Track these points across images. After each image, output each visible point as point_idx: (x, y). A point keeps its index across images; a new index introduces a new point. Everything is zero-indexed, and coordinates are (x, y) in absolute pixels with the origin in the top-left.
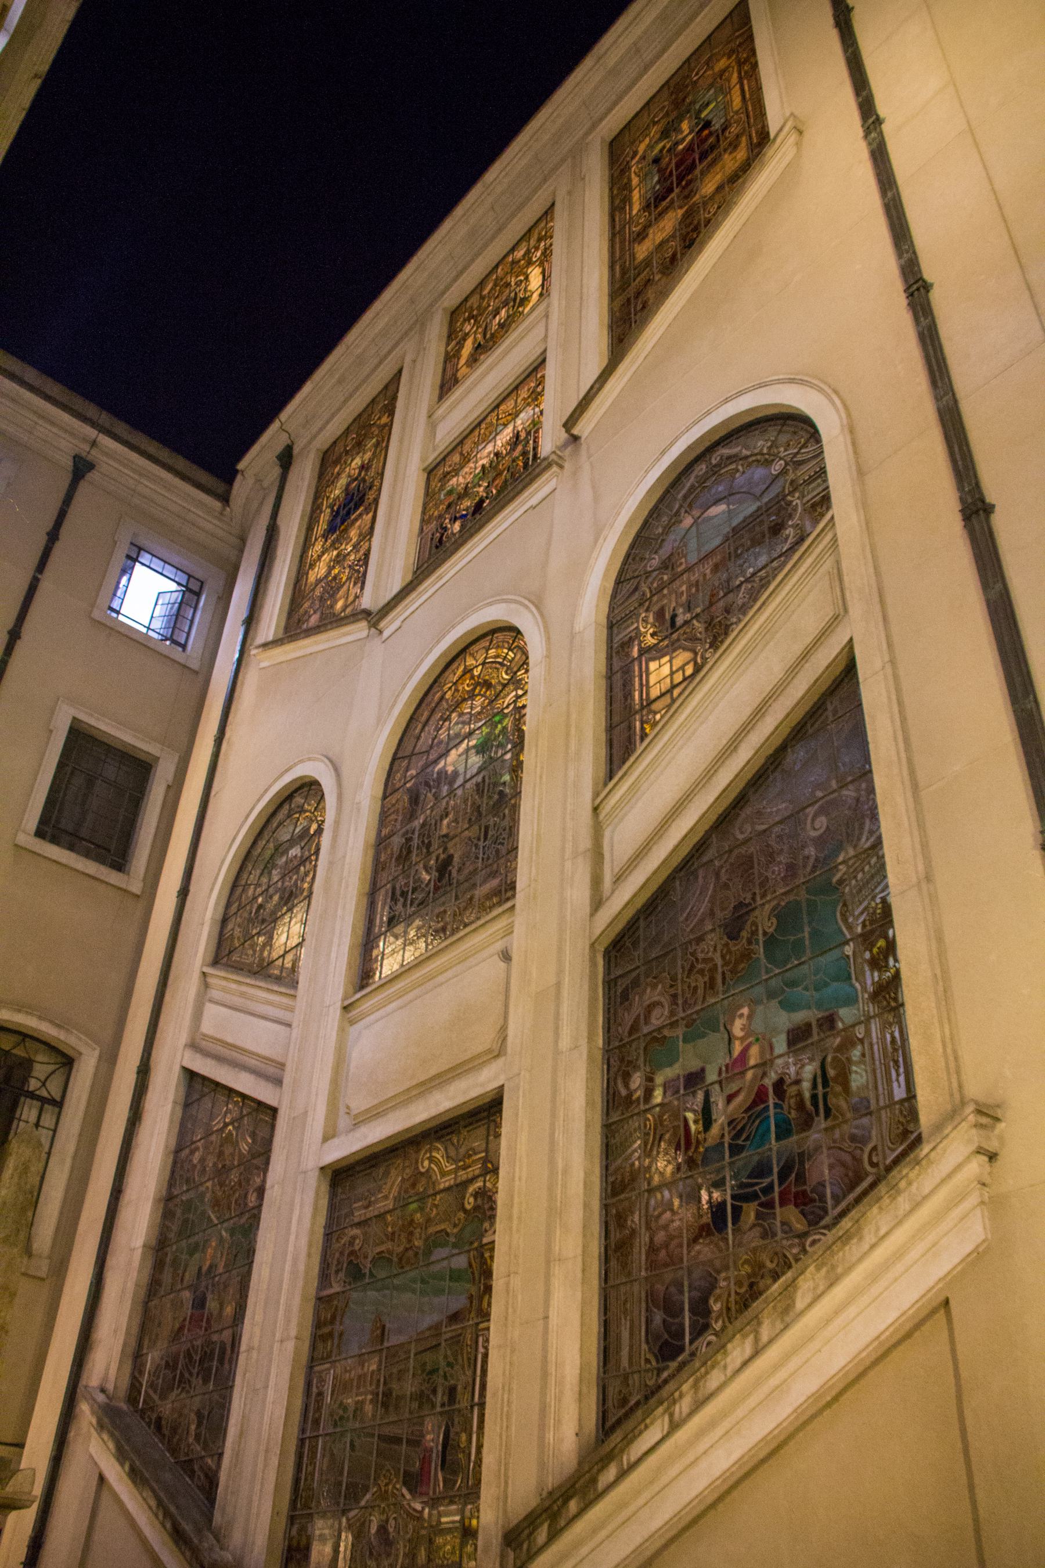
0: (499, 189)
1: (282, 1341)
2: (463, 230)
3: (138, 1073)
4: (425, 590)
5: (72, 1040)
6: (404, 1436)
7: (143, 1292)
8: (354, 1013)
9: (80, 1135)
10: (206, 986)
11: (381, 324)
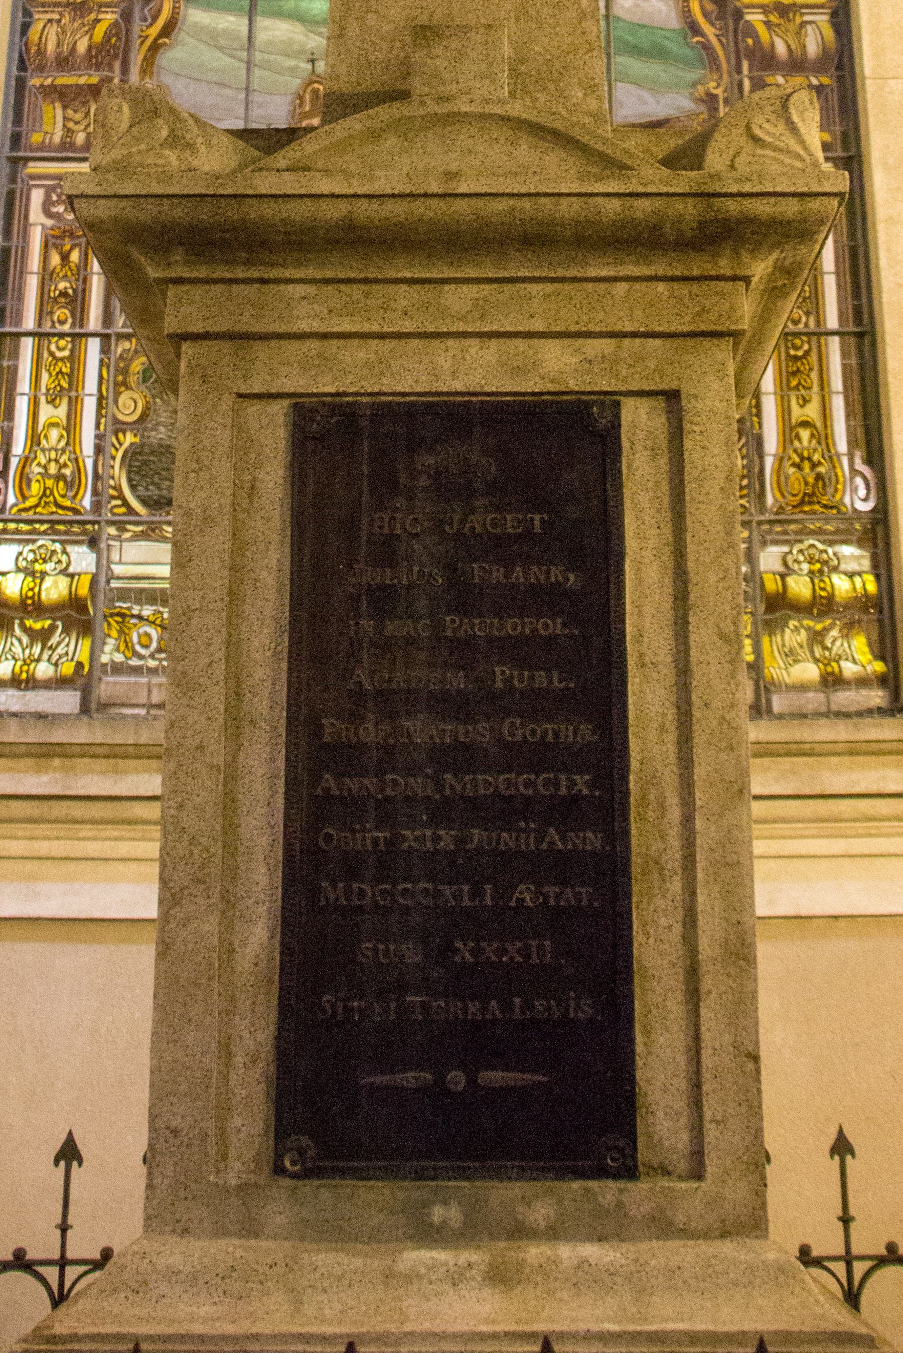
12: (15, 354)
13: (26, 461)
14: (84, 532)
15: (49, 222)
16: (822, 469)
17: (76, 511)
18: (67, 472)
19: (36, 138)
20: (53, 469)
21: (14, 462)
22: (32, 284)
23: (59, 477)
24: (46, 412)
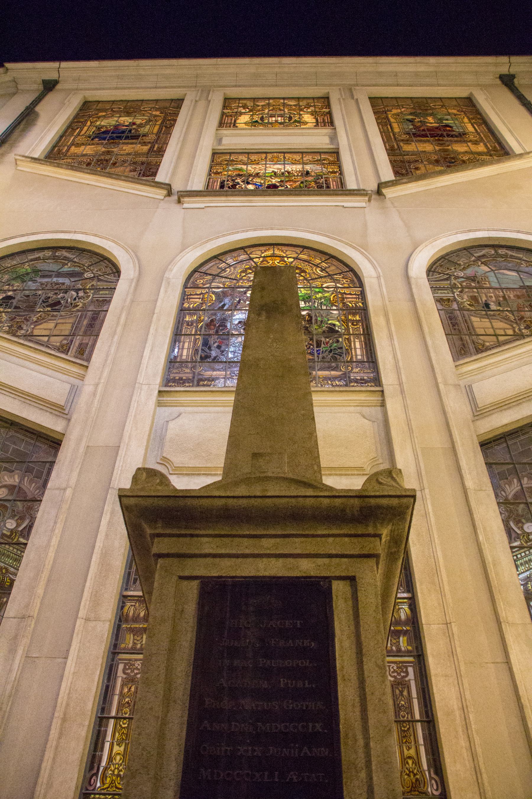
0: (286, 70)
2: (253, 70)
4: (234, 201)
8: (166, 398)
11: (168, 71)
12: (107, 726)
13: (106, 769)
15: (125, 676)
16: (418, 777)
19: (123, 646)
20: (116, 772)
21: (101, 769)
22: (116, 698)
23: (118, 775)
24: (116, 749)
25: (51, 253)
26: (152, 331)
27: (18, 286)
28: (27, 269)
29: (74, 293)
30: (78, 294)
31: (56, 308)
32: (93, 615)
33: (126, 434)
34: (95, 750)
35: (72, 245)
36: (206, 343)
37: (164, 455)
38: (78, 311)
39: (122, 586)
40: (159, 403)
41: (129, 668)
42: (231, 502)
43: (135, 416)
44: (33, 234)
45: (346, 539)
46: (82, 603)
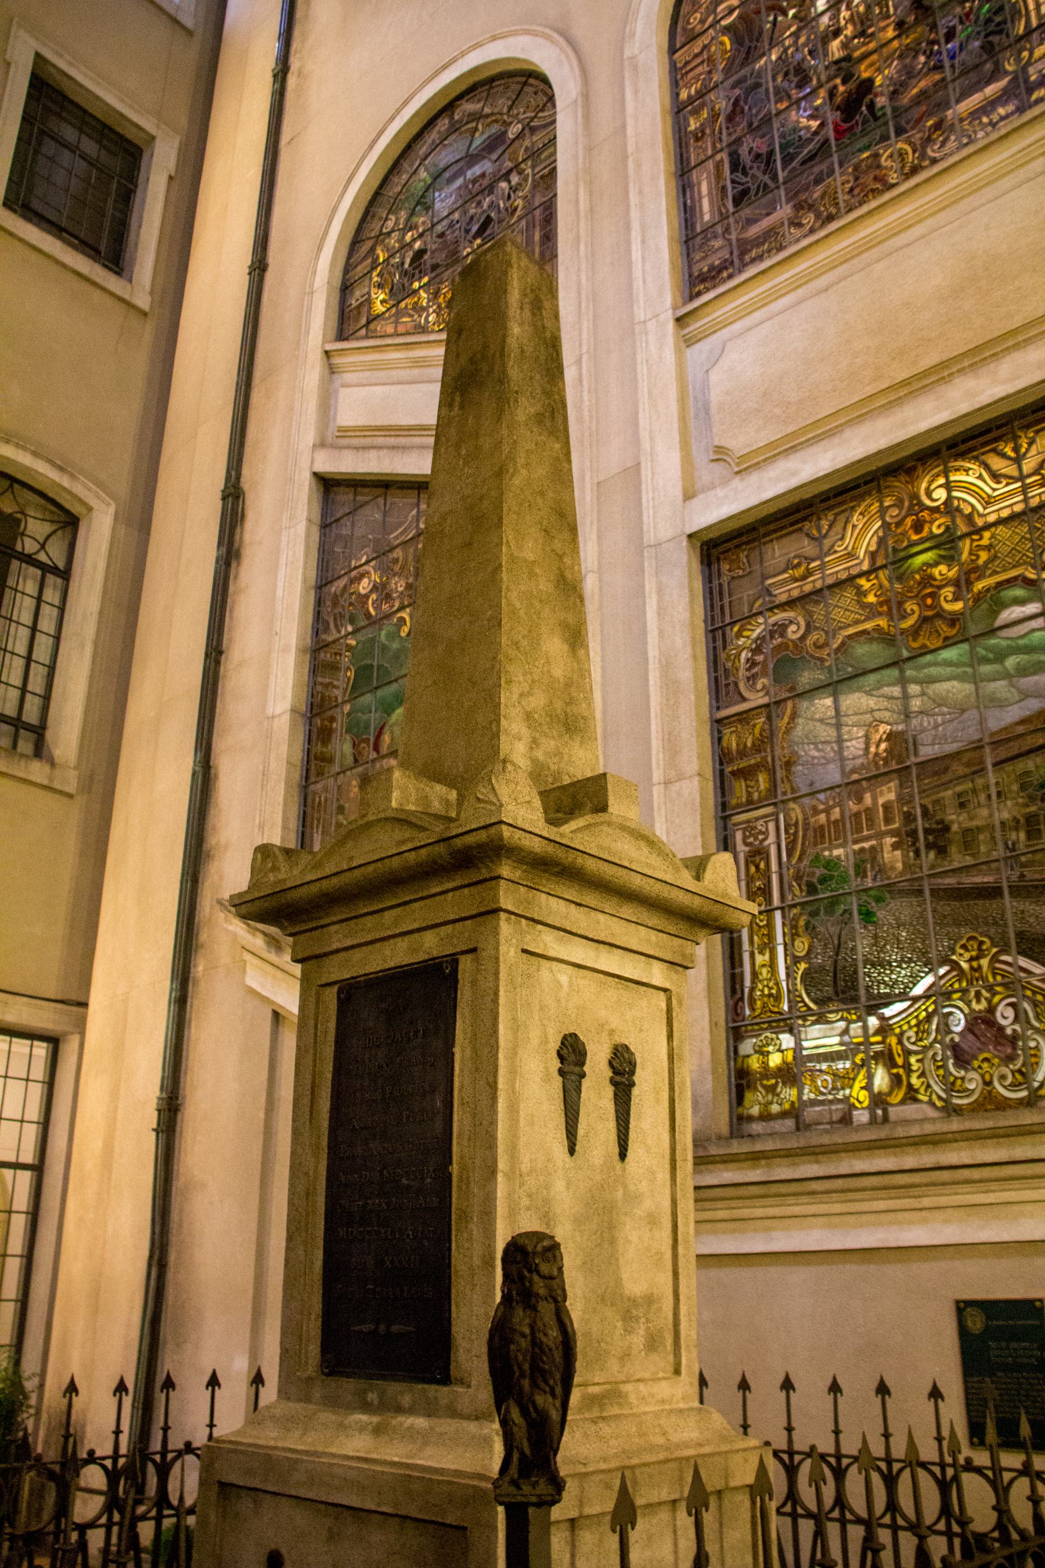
1: (667, 783)
3: (224, 499)
5: (78, 489)
6: (1005, 885)
7: (297, 775)
8: (695, 326)
9: (101, 613)
10: (332, 370)
13: (752, 989)
14: (786, 1025)
15: (747, 849)
17: (780, 1013)
18: (774, 991)
19: (734, 802)
20: (766, 991)
21: (746, 991)
23: (770, 995)
24: (760, 959)
25: (447, 121)
26: (633, 198)
27: (424, 223)
28: (424, 180)
29: (504, 185)
30: (509, 182)
31: (488, 232)
32: (673, 773)
33: (644, 435)
34: (733, 967)
35: (470, 81)
36: (736, 165)
37: (717, 443)
38: (520, 219)
39: (711, 706)
40: (685, 341)
41: (751, 835)
42: (325, 885)
43: (650, 393)
44: (405, 103)
45: (466, 891)
46: (654, 760)
